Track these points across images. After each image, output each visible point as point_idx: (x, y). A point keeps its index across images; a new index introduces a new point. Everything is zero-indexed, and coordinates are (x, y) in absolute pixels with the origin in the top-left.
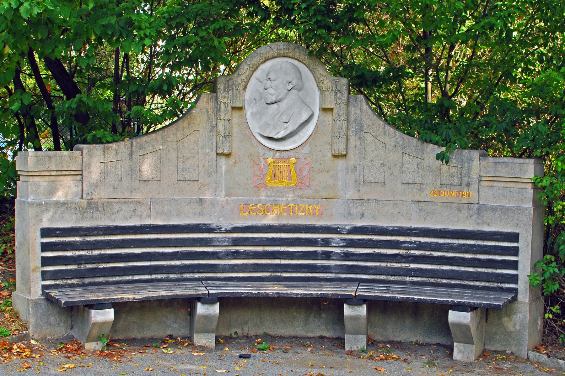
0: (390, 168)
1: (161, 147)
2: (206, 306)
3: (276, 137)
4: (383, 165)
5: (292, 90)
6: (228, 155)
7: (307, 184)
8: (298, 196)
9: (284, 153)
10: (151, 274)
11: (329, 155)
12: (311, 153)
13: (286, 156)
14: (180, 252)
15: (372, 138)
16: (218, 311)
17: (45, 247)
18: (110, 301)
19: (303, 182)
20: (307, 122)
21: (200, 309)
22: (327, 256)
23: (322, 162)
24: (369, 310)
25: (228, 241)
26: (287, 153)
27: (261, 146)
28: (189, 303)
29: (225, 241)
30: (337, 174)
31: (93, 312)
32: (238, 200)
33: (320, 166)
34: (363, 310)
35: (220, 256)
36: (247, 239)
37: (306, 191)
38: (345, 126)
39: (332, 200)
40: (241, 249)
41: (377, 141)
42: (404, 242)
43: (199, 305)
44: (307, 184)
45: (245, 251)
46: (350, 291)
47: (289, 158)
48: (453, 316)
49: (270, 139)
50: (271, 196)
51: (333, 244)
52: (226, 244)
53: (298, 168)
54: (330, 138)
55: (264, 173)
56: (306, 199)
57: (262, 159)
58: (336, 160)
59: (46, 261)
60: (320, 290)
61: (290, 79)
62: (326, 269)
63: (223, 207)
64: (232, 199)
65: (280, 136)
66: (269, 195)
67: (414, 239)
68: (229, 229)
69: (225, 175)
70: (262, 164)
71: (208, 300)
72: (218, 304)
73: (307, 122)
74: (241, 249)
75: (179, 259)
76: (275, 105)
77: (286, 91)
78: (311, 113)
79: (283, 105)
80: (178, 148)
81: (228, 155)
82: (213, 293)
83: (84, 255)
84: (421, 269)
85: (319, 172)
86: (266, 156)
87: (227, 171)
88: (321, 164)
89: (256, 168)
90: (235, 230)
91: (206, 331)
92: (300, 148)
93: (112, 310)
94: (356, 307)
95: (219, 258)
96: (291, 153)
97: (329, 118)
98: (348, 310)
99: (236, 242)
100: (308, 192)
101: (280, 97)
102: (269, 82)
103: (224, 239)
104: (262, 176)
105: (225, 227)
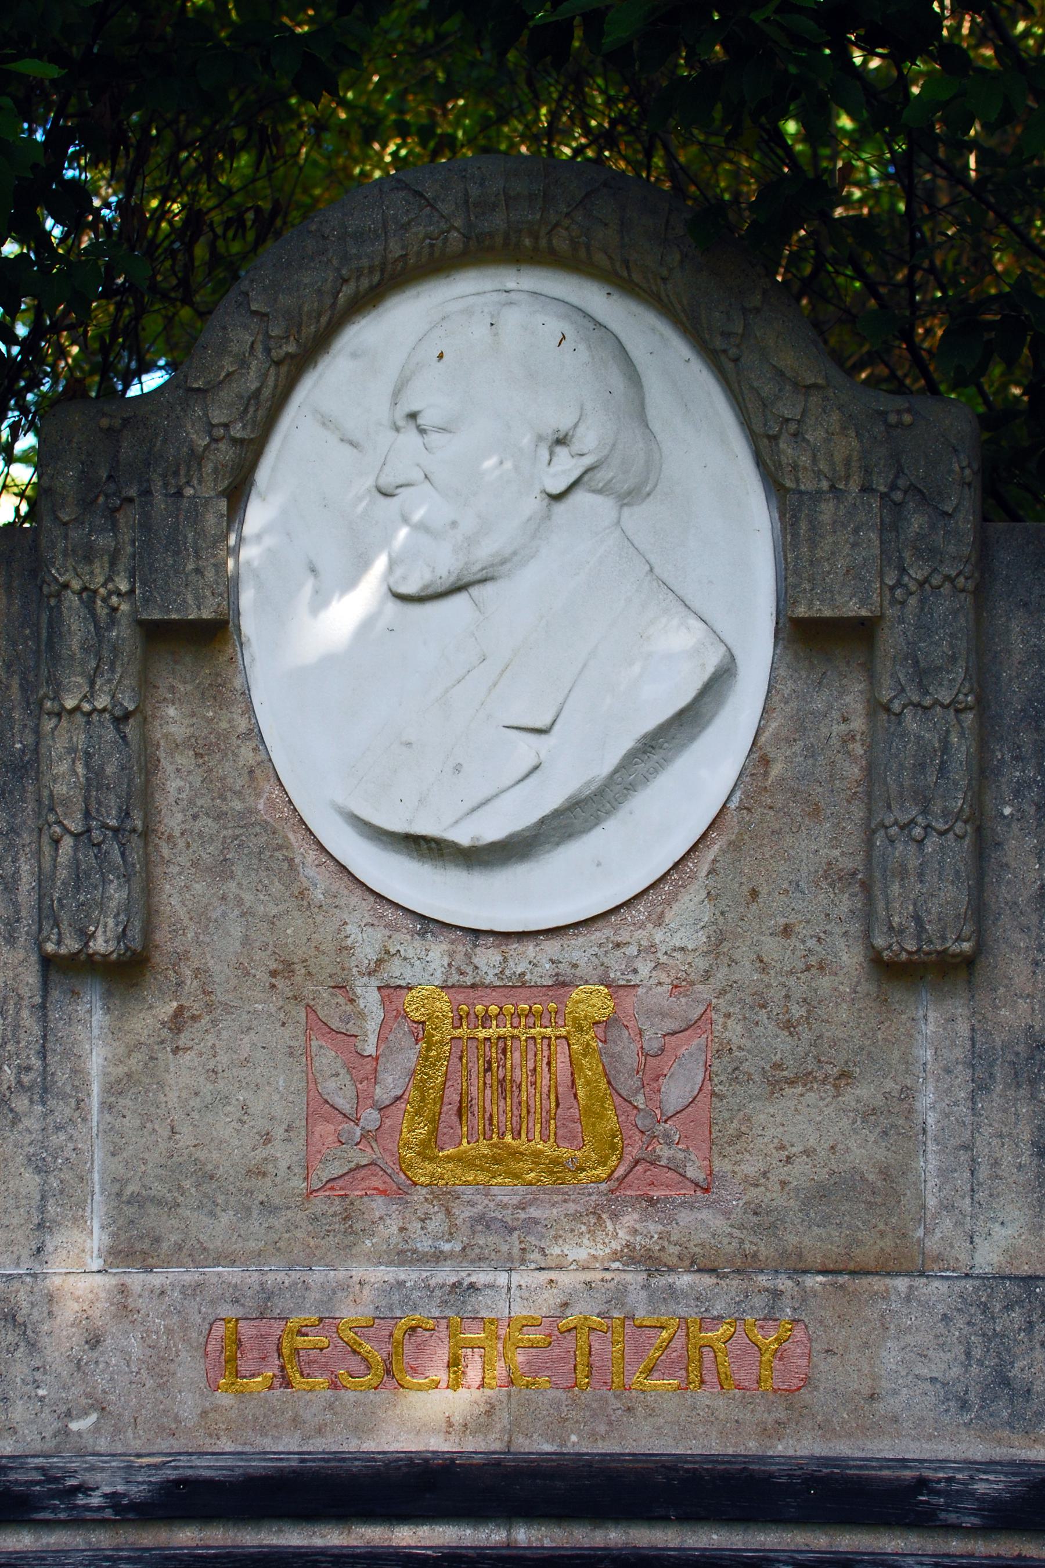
3: (463, 836)
7: (691, 1172)
9: (530, 949)
11: (850, 958)
12: (718, 943)
13: (543, 974)
19: (664, 1152)
20: (688, 721)
23: (798, 1011)
26: (552, 947)
27: (356, 899)
30: (907, 1094)
32: (198, 1287)
33: (783, 1043)
37: (685, 1217)
38: (961, 748)
39: (878, 1283)
47: (562, 984)
50: (438, 1257)
54: (855, 840)
56: (684, 1280)
57: (369, 997)
64: (156, 1279)
66: (424, 1245)
68: (137, 1491)
69: (107, 1107)
70: (372, 1026)
73: (688, 721)
76: (460, 600)
77: (533, 504)
78: (713, 660)
85: (777, 1080)
86: (396, 970)
87: (115, 1088)
88: (789, 1026)
89: (327, 1058)
92: (640, 912)
96: (579, 951)
101: (485, 551)
102: (410, 437)
104: (370, 1117)
105: (107, 1483)
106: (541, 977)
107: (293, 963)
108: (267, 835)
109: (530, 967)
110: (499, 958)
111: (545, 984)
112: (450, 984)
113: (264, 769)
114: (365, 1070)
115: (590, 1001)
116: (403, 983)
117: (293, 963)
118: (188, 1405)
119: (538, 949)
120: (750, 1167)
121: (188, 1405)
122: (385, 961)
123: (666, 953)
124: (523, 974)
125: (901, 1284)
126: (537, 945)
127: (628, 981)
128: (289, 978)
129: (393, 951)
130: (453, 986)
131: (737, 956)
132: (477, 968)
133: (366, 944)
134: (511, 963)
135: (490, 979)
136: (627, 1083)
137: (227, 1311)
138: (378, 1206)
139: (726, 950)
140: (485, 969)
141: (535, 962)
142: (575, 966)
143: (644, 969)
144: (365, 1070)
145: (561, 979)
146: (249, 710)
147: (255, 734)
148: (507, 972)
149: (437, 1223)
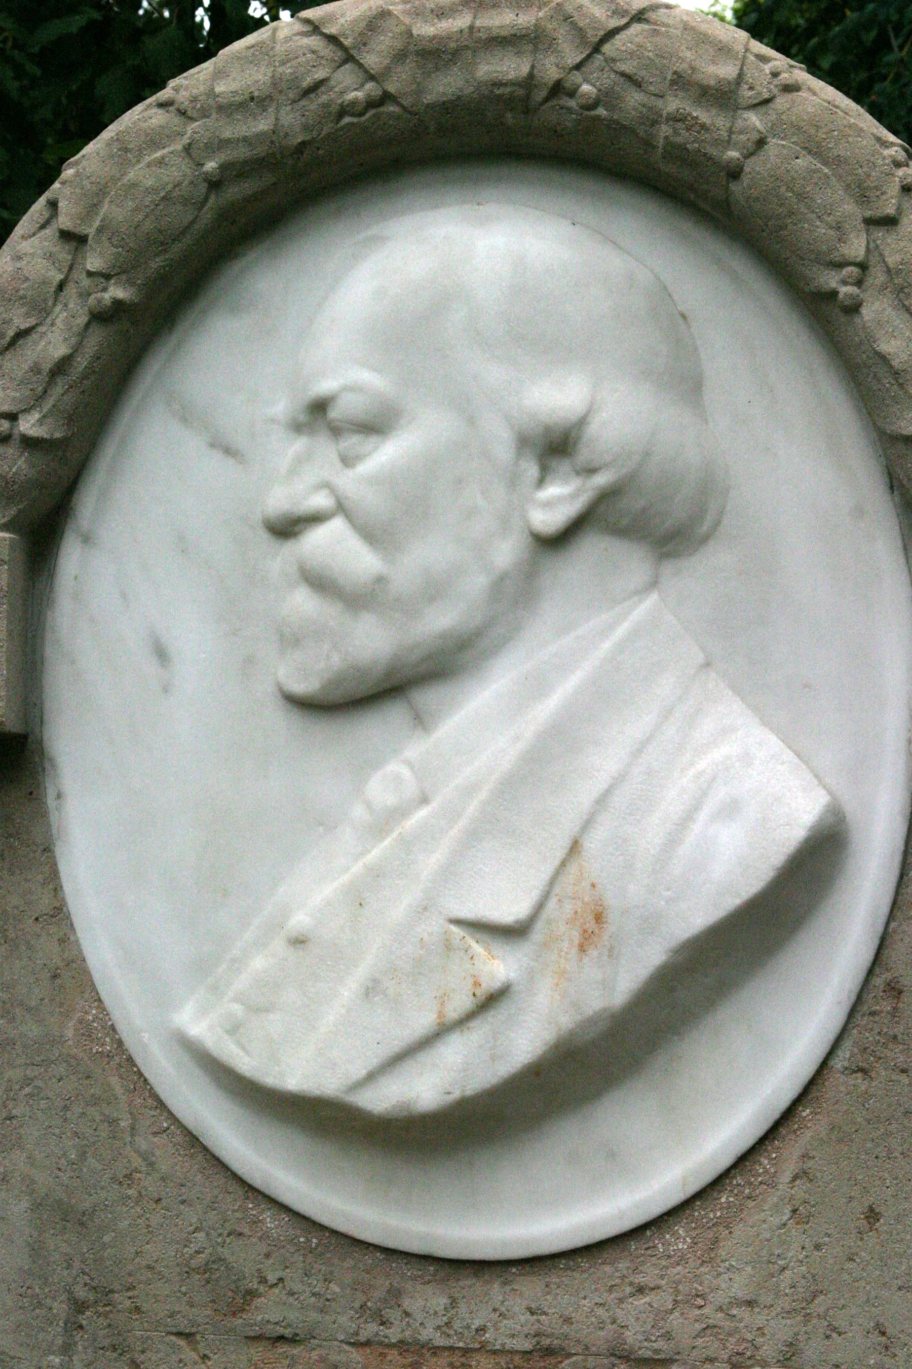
3: (381, 1099)
5: (593, 548)
26: (530, 1288)
49: (323, 1121)
61: (557, 396)
65: (425, 1087)
77: (507, 552)
79: (481, 726)
92: (680, 1238)
101: (441, 620)
106: (513, 1336)
107: (112, 1291)
109: (495, 1316)
110: (443, 1301)
111: (518, 1347)
112: (362, 1338)
113: (71, 976)
116: (287, 1332)
117: (112, 1291)
119: (508, 1288)
122: (260, 1295)
123: (720, 1309)
124: (482, 1329)
126: (504, 1284)
127: (657, 1351)
128: (106, 1315)
129: (272, 1278)
130: (368, 1343)
131: (841, 1323)
132: (407, 1314)
134: (463, 1308)
135: (428, 1334)
139: (821, 1310)
140: (419, 1316)
142: (568, 1320)
145: (546, 1342)
146: (53, 879)
147: (59, 913)
148: (457, 1325)
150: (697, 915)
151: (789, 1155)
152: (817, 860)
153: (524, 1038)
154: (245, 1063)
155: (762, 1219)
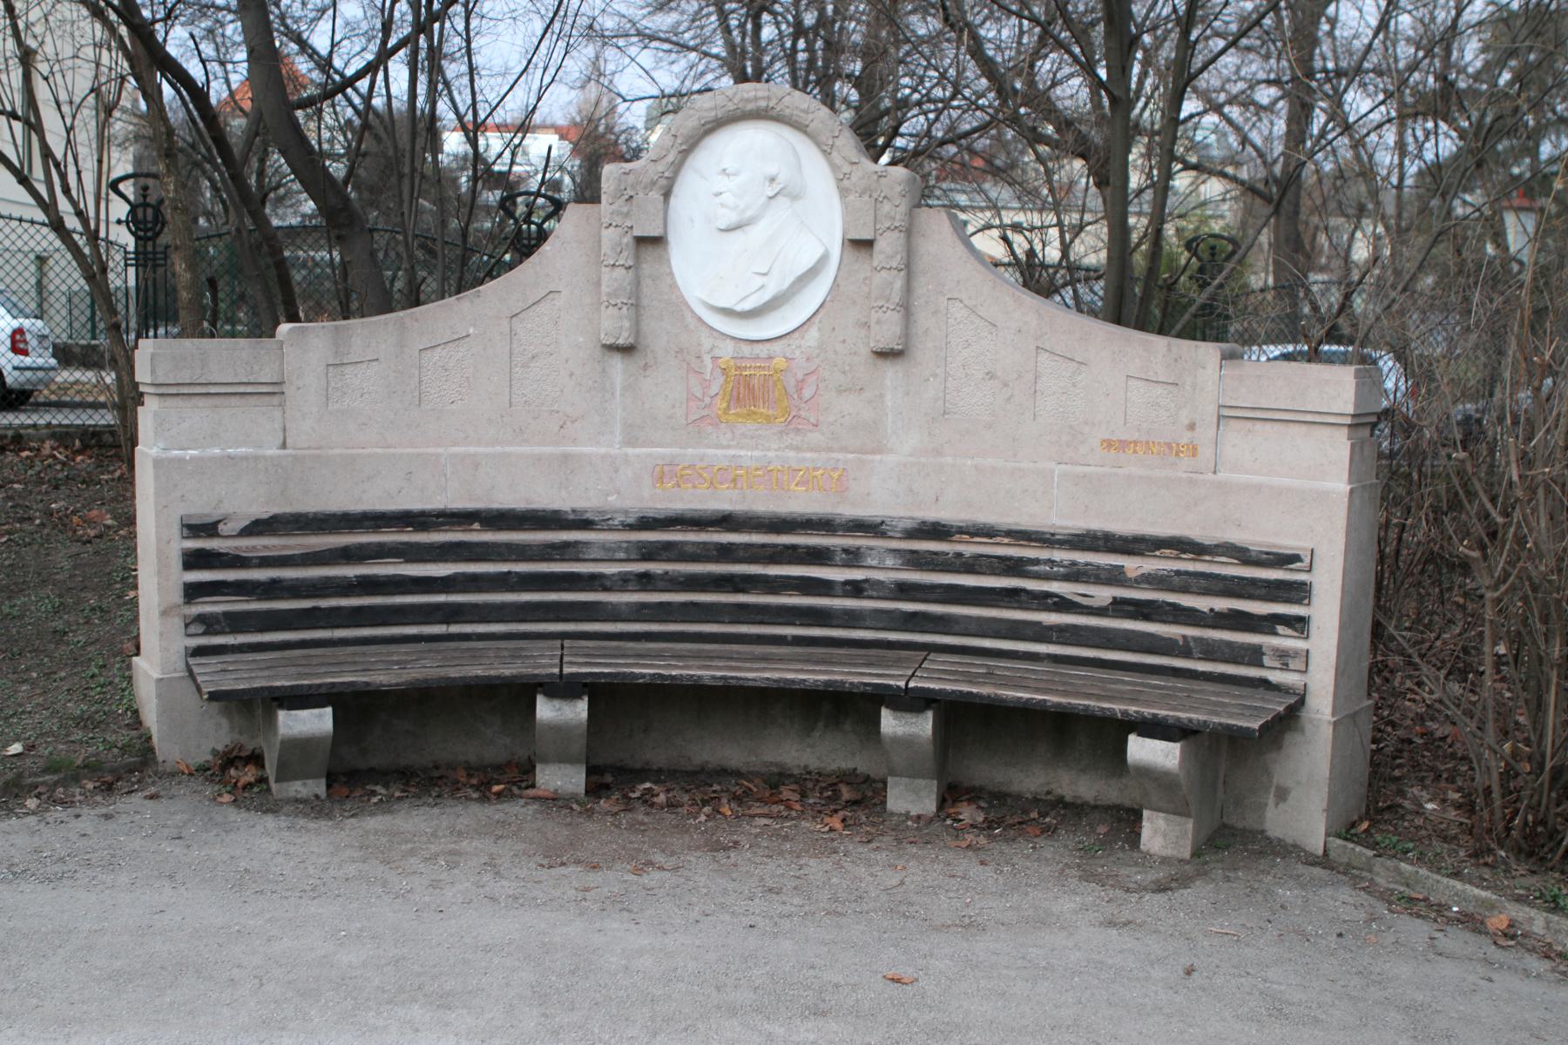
0: (1006, 385)
1: (471, 331)
2: (557, 703)
3: (739, 308)
4: (991, 375)
5: (780, 199)
6: (627, 350)
7: (812, 420)
8: (790, 447)
9: (760, 346)
10: (448, 623)
14: (517, 573)
15: (965, 312)
16: (585, 715)
17: (193, 560)
18: (323, 691)
19: (803, 413)
21: (546, 710)
22: (856, 589)
24: (941, 727)
25: (627, 550)
26: (768, 345)
28: (521, 694)
29: (620, 548)
30: (881, 396)
31: (282, 715)
34: (923, 726)
35: (608, 583)
36: (668, 546)
39: (871, 457)
40: (656, 568)
41: (977, 321)
42: (1037, 562)
43: (541, 702)
44: (812, 420)
45: (666, 573)
46: (896, 679)
48: (1141, 749)
49: (728, 312)
50: (728, 447)
51: (870, 562)
52: (622, 555)
53: (792, 382)
55: (712, 392)
58: (880, 362)
59: (193, 592)
60: (825, 672)
61: (772, 169)
62: (852, 619)
63: (616, 471)
64: (638, 451)
65: (747, 306)
67: (1059, 555)
68: (630, 520)
70: (709, 369)
71: (564, 688)
72: (586, 698)
74: (656, 568)
75: (512, 590)
77: (763, 199)
79: (756, 233)
80: (512, 333)
81: (627, 350)
82: (571, 674)
83: (271, 580)
84: (1075, 627)
85: (840, 391)
86: (717, 353)
89: (693, 380)
90: (646, 523)
91: (564, 758)
92: (796, 335)
93: (329, 710)
94: (908, 716)
95: (606, 589)
96: (777, 347)
97: (861, 266)
98: (890, 723)
99: (649, 553)
100: (815, 437)
101: (749, 214)
103: (618, 546)
104: (707, 400)
108: (679, 306)
113: (674, 286)
114: (705, 384)
115: (779, 362)
118: (646, 493)
120: (831, 419)
121: (646, 493)
125: (878, 457)
133: (707, 343)
136: (792, 390)
137: (660, 462)
138: (710, 429)
141: (762, 350)
143: (798, 353)
144: (705, 384)
146: (670, 266)
147: (671, 274)
149: (729, 435)
150: (800, 272)
151: (817, 319)
152: (823, 260)
153: (766, 296)
154: (712, 302)
155: (813, 333)
